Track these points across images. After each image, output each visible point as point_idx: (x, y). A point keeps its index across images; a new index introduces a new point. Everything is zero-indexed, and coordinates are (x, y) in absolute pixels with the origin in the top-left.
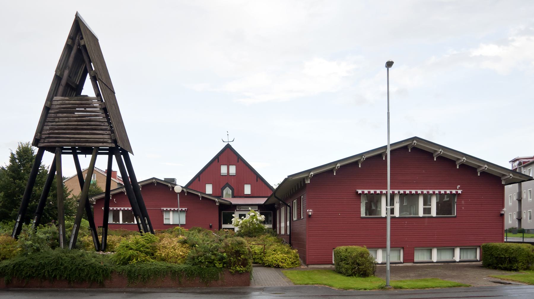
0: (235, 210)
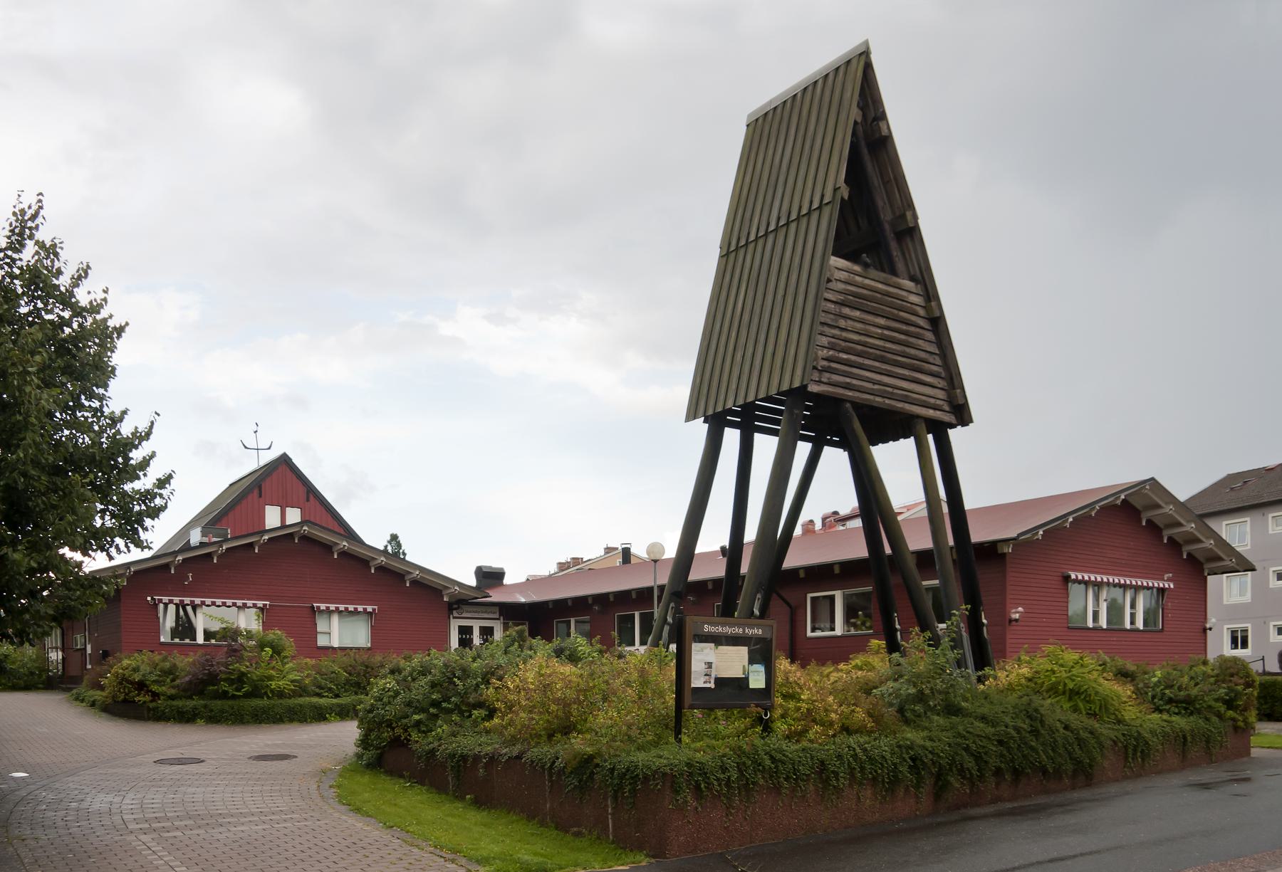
0: (451, 616)
